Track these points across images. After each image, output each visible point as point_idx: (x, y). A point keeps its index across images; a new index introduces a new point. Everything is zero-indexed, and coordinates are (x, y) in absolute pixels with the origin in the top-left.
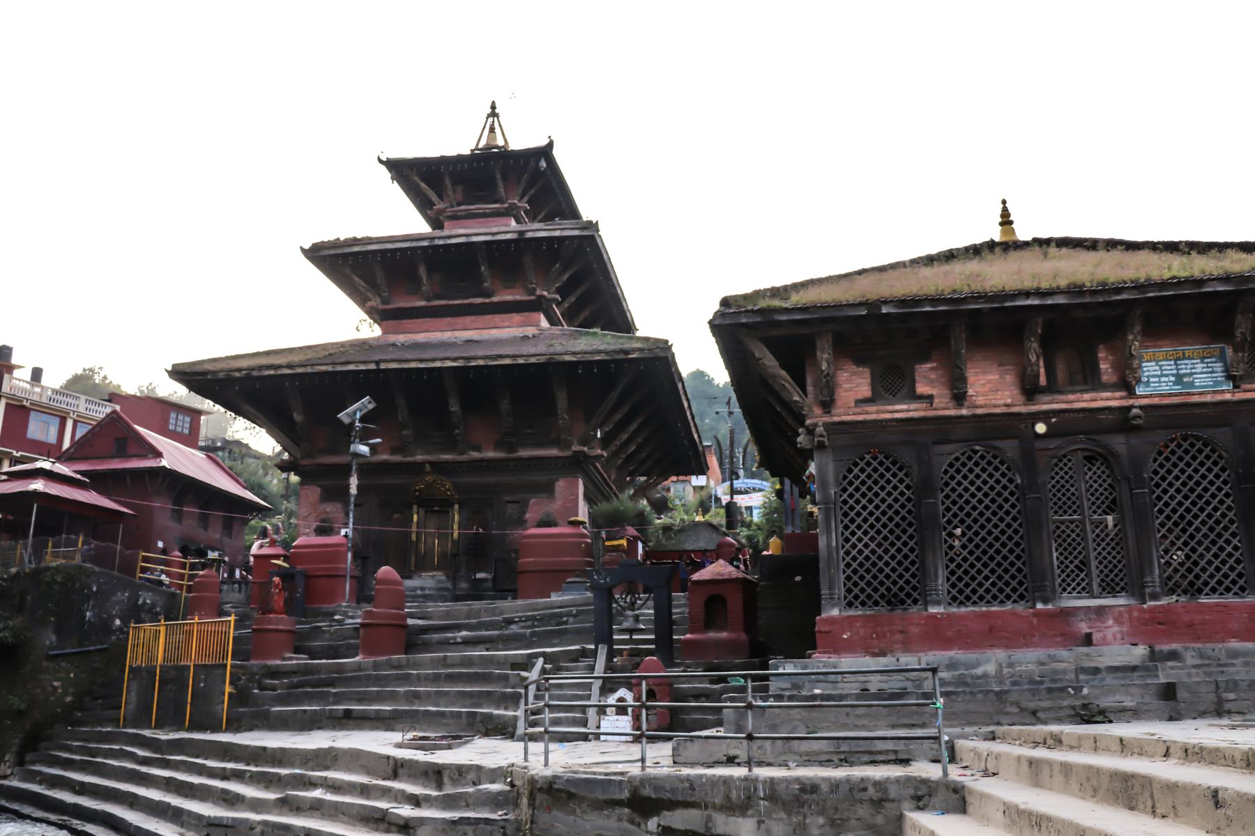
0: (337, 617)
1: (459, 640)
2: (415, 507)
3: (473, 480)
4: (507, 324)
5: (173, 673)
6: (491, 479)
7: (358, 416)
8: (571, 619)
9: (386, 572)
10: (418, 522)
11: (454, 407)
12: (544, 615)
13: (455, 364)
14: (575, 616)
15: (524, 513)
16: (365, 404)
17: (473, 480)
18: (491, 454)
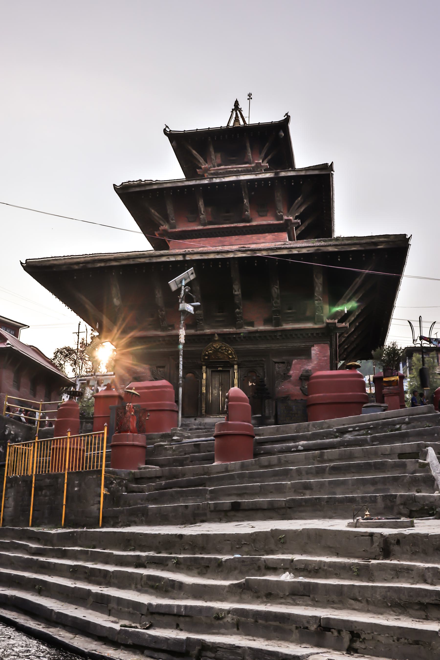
0: (175, 438)
1: (300, 448)
2: (204, 367)
3: (250, 347)
4: (262, 241)
5: (48, 481)
6: (262, 346)
7: (184, 283)
8: (404, 426)
9: (235, 391)
10: (207, 379)
11: (237, 291)
12: (378, 424)
13: (244, 255)
14: (407, 423)
15: (289, 370)
16: (189, 274)
17: (250, 347)
18: (262, 328)
